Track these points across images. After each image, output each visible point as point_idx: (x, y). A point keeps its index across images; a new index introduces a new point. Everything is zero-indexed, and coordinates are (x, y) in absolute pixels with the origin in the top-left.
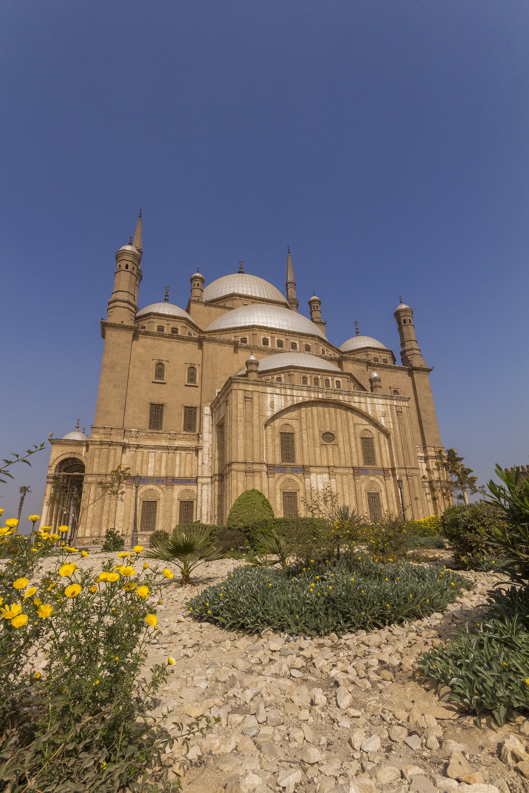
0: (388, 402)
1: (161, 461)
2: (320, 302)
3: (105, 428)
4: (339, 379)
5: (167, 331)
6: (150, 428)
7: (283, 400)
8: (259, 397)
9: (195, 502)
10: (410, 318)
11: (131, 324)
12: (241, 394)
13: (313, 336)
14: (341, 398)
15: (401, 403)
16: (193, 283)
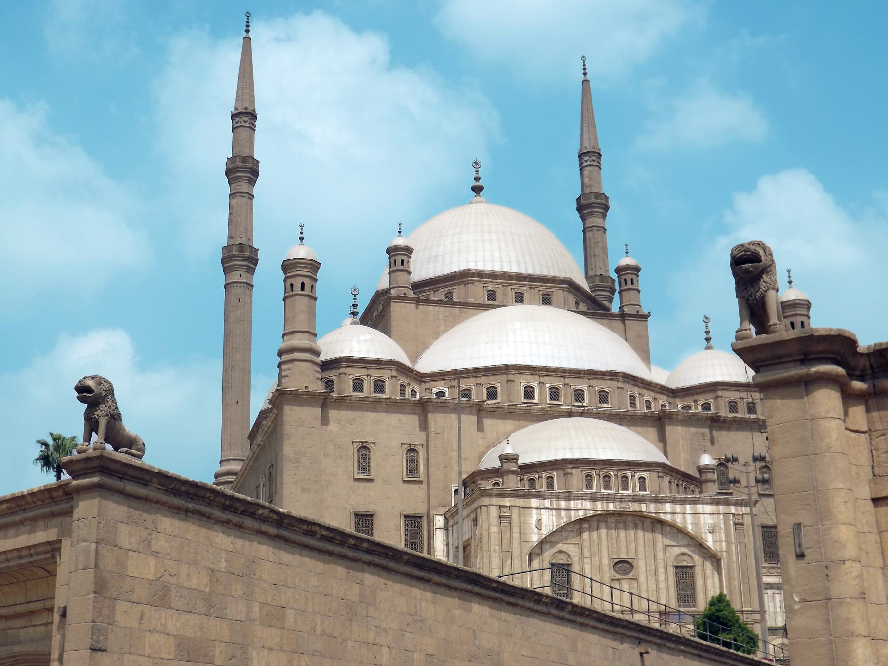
0: (722, 508)
2: (637, 269)
4: (644, 474)
7: (554, 517)
8: (520, 514)
10: (804, 319)
11: (317, 387)
12: (494, 511)
13: (613, 375)
14: (644, 507)
15: (745, 510)
16: (393, 259)
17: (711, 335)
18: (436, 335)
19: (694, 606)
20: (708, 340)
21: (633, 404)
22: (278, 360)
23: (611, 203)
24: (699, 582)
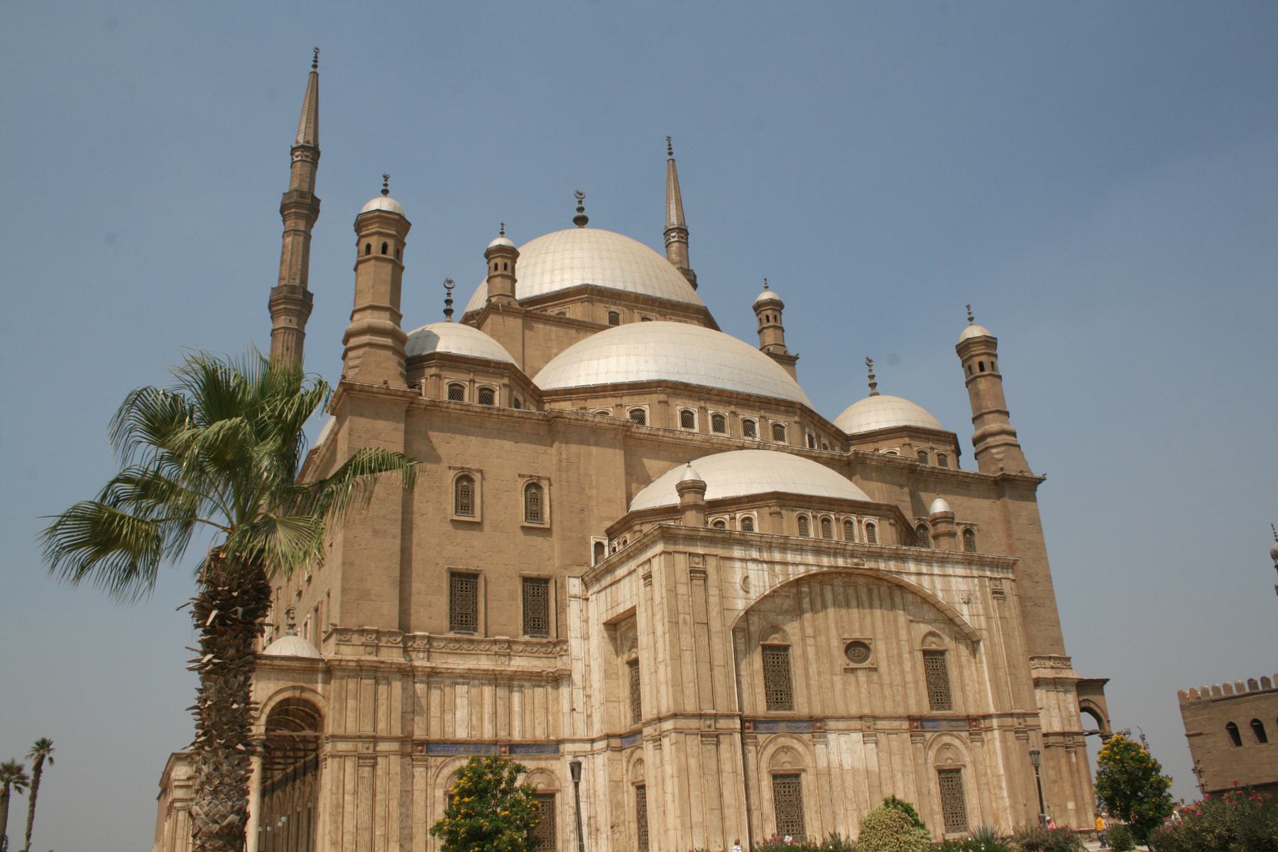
1: (482, 705)
3: (363, 631)
4: (873, 520)
5: (470, 396)
6: (452, 629)
8: (718, 569)
9: (558, 796)
10: (993, 359)
14: (882, 565)
16: (493, 262)
17: (875, 380)
18: (561, 350)
19: (950, 708)
20: (873, 385)
21: (811, 445)
22: (343, 348)
23: (698, 281)
24: (953, 674)
